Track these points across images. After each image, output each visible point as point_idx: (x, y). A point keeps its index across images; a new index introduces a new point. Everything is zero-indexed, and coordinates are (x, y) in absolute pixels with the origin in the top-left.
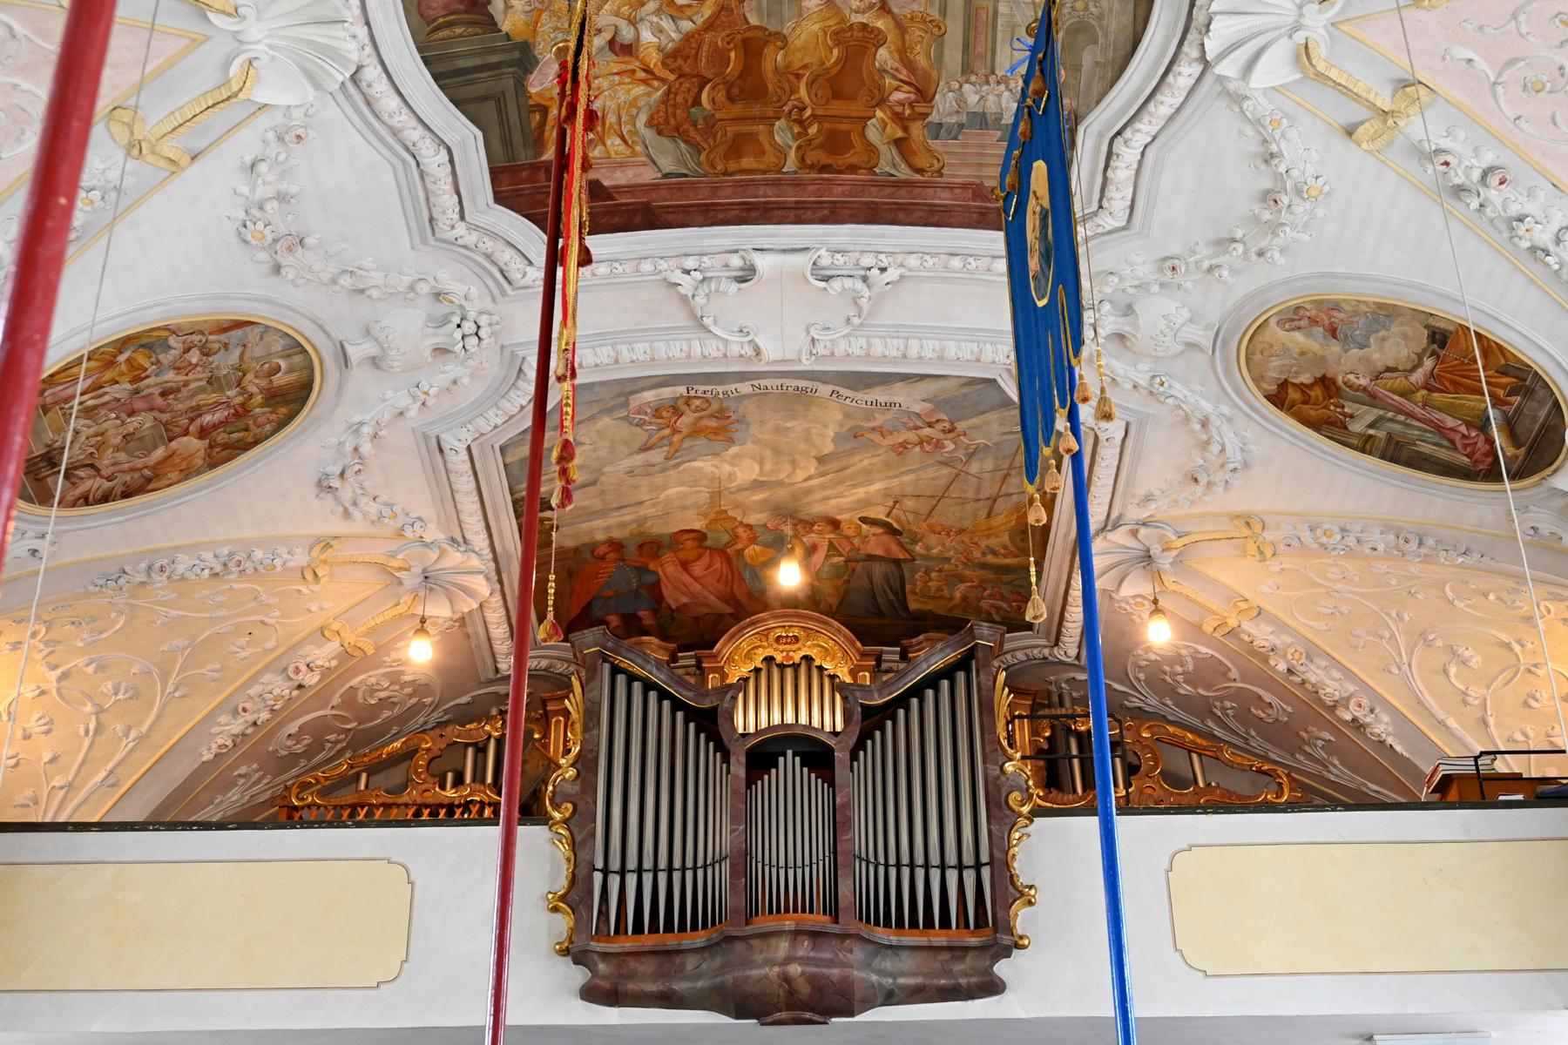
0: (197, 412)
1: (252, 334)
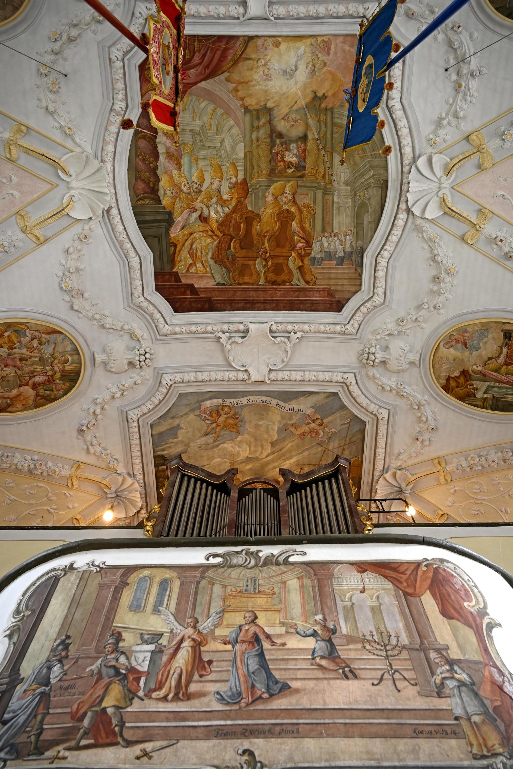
0: (33, 374)
1: (60, 337)
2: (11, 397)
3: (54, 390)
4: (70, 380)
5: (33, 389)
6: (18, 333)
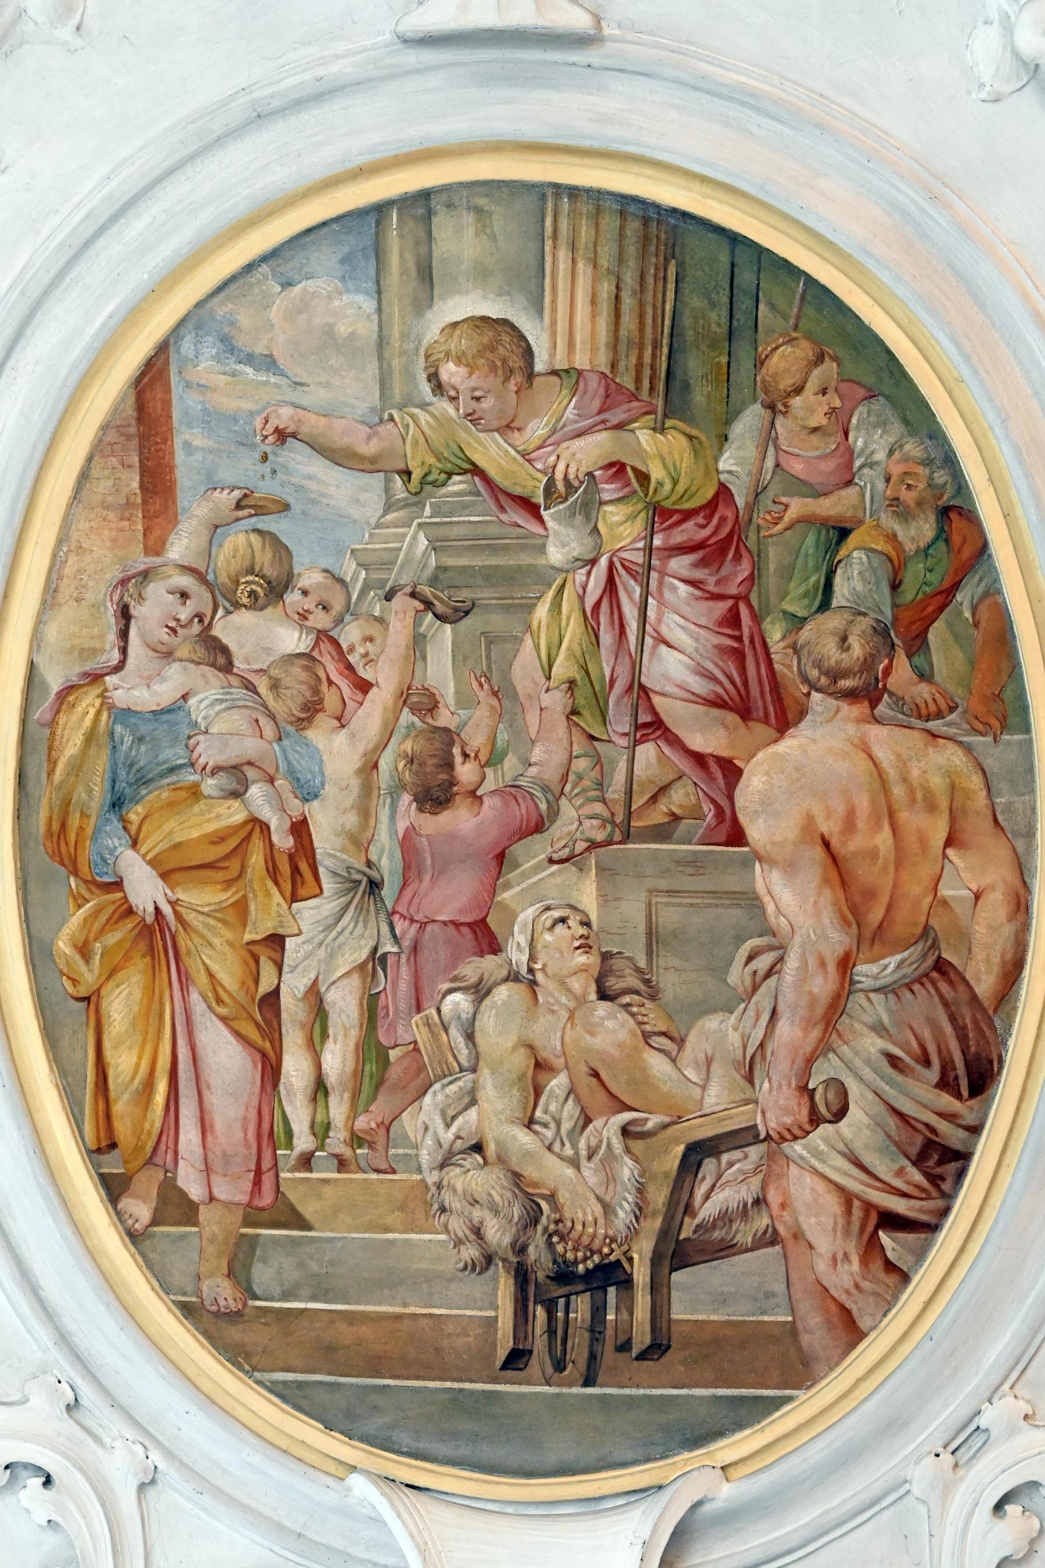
1: (205, 385)
2: (837, 940)
3: (831, 506)
4: (738, 331)
5: (784, 718)
6: (143, 781)
